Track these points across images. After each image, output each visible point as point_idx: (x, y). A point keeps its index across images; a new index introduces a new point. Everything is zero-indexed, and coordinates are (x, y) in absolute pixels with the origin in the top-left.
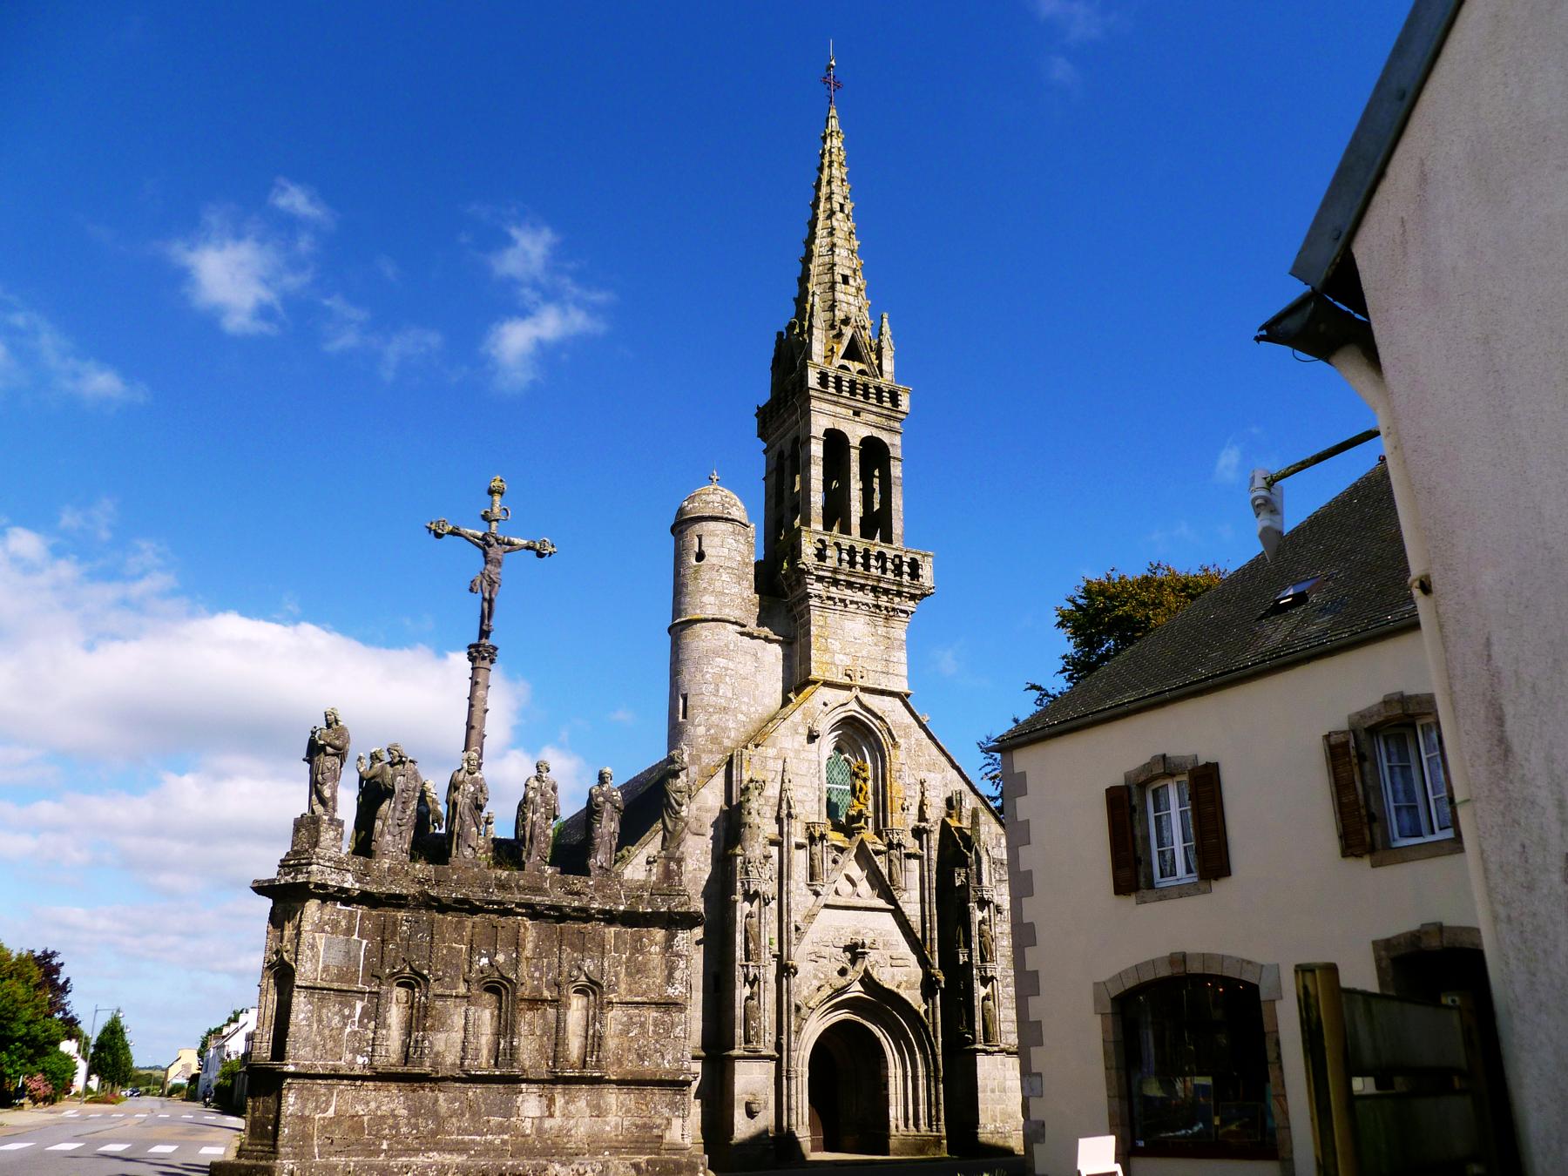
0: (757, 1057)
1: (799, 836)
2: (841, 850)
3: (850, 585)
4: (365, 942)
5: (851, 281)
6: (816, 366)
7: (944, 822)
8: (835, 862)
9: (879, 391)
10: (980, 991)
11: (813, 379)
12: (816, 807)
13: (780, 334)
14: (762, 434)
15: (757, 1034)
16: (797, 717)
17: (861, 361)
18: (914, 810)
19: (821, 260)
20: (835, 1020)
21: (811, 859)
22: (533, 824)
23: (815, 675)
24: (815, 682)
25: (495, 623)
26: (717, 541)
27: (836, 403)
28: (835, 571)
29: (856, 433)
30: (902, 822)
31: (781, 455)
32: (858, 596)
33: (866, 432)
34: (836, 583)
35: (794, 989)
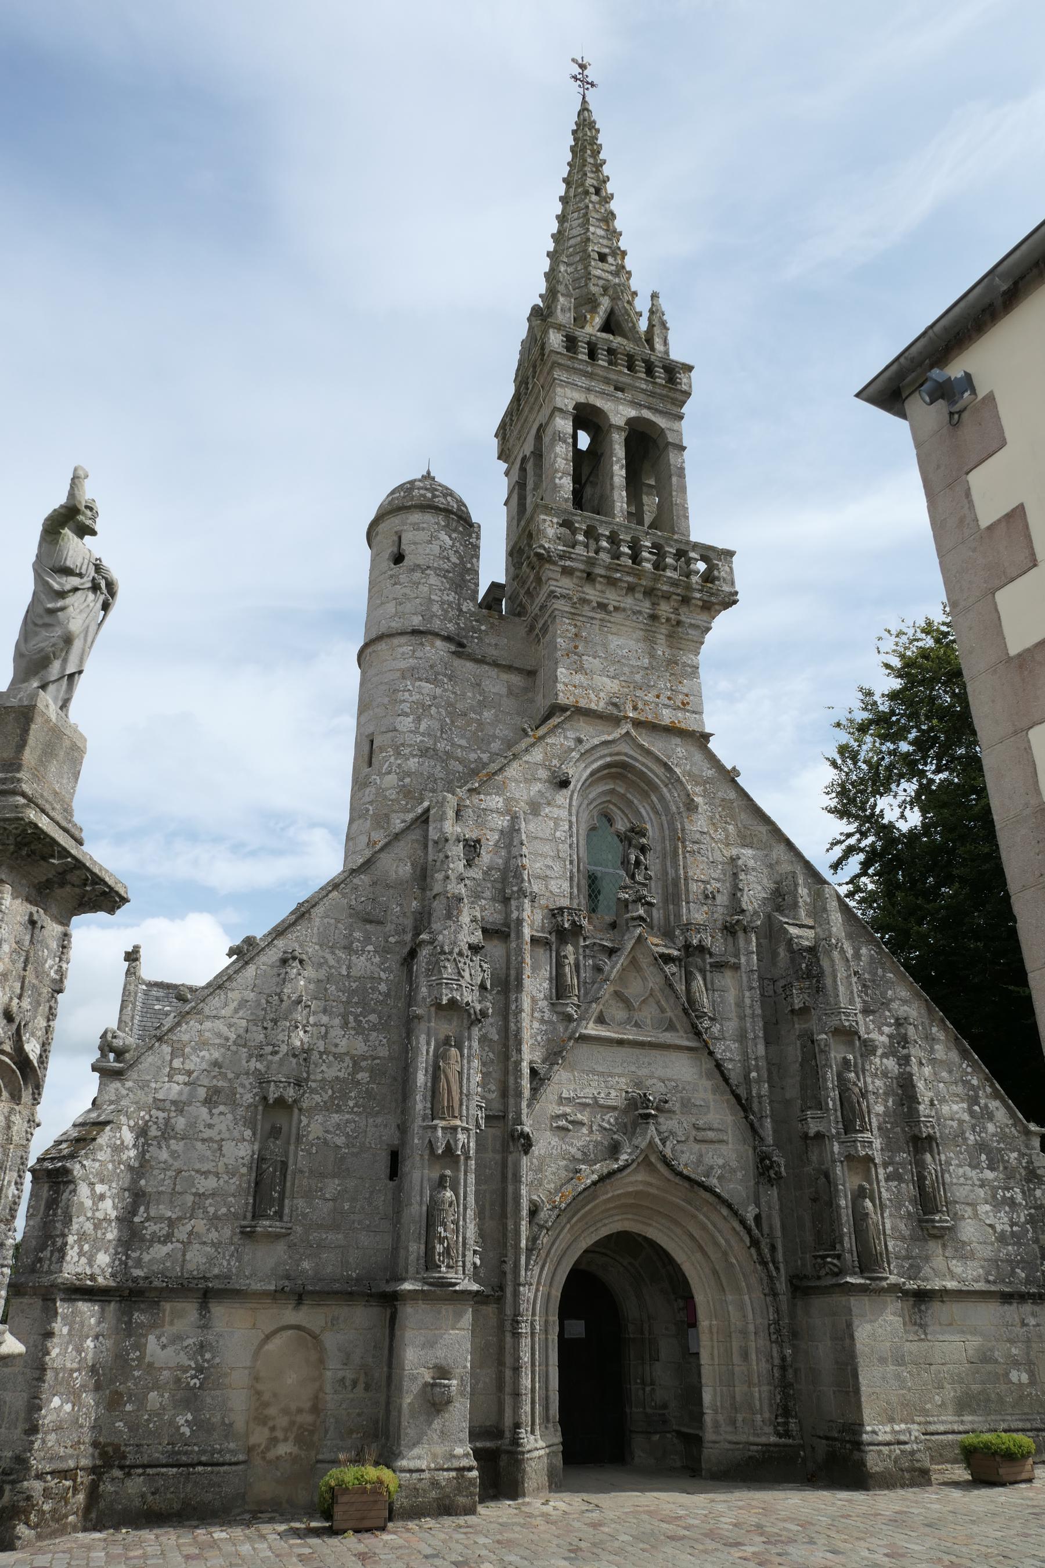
0: (442, 1293)
1: (532, 921)
3: (612, 582)
5: (610, 259)
6: (559, 327)
7: (769, 917)
10: (847, 1182)
12: (566, 885)
15: (447, 1251)
16: (537, 755)
17: (625, 336)
18: (722, 899)
20: (604, 1232)
21: (559, 966)
23: (562, 699)
27: (590, 376)
28: (591, 562)
29: (619, 413)
32: (628, 602)
33: (633, 413)
34: (590, 577)
35: (527, 1175)
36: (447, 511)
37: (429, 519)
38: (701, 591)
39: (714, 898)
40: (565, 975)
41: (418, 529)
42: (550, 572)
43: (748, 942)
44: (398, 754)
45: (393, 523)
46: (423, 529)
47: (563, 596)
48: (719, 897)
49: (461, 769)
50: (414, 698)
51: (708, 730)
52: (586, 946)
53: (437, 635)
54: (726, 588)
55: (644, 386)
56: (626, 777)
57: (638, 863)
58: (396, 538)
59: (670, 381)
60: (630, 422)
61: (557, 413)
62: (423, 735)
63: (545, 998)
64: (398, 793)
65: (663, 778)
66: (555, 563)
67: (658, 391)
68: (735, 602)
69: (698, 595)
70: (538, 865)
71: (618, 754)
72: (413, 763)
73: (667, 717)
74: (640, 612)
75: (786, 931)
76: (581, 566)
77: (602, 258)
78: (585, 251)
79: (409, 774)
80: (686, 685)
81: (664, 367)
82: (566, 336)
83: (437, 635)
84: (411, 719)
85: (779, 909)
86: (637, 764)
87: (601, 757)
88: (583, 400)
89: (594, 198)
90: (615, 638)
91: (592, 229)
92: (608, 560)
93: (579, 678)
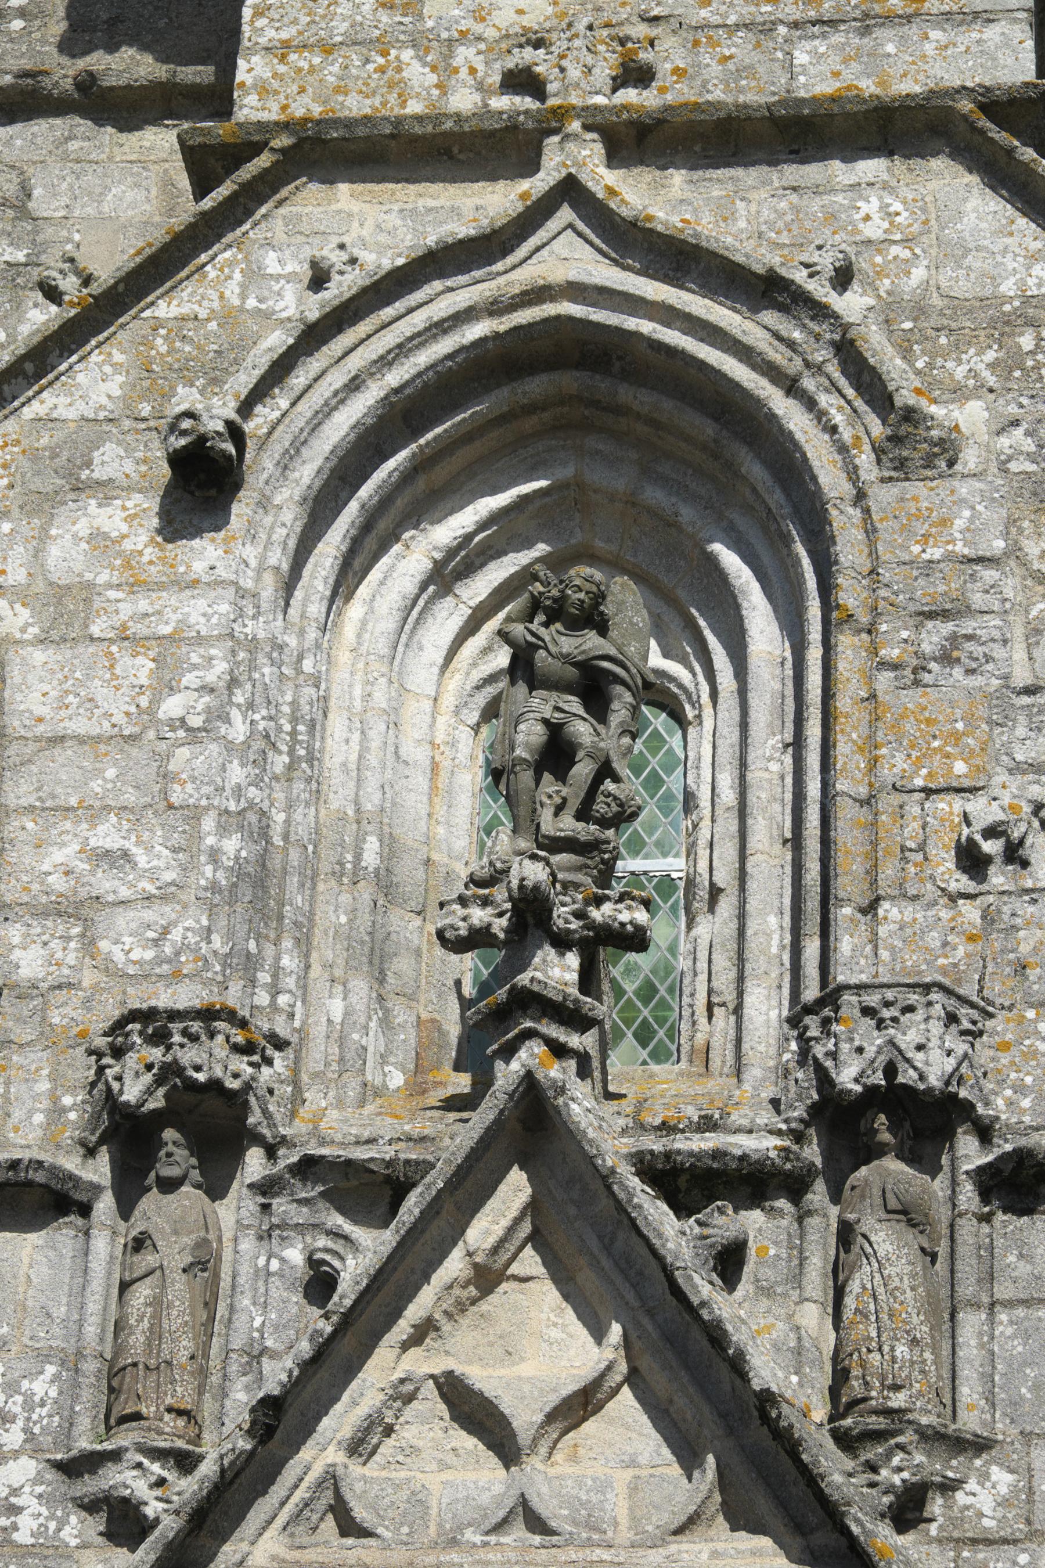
56: (620, 411)
63: (32, 1445)
65: (777, 355)
70: (58, 856)
86: (632, 323)
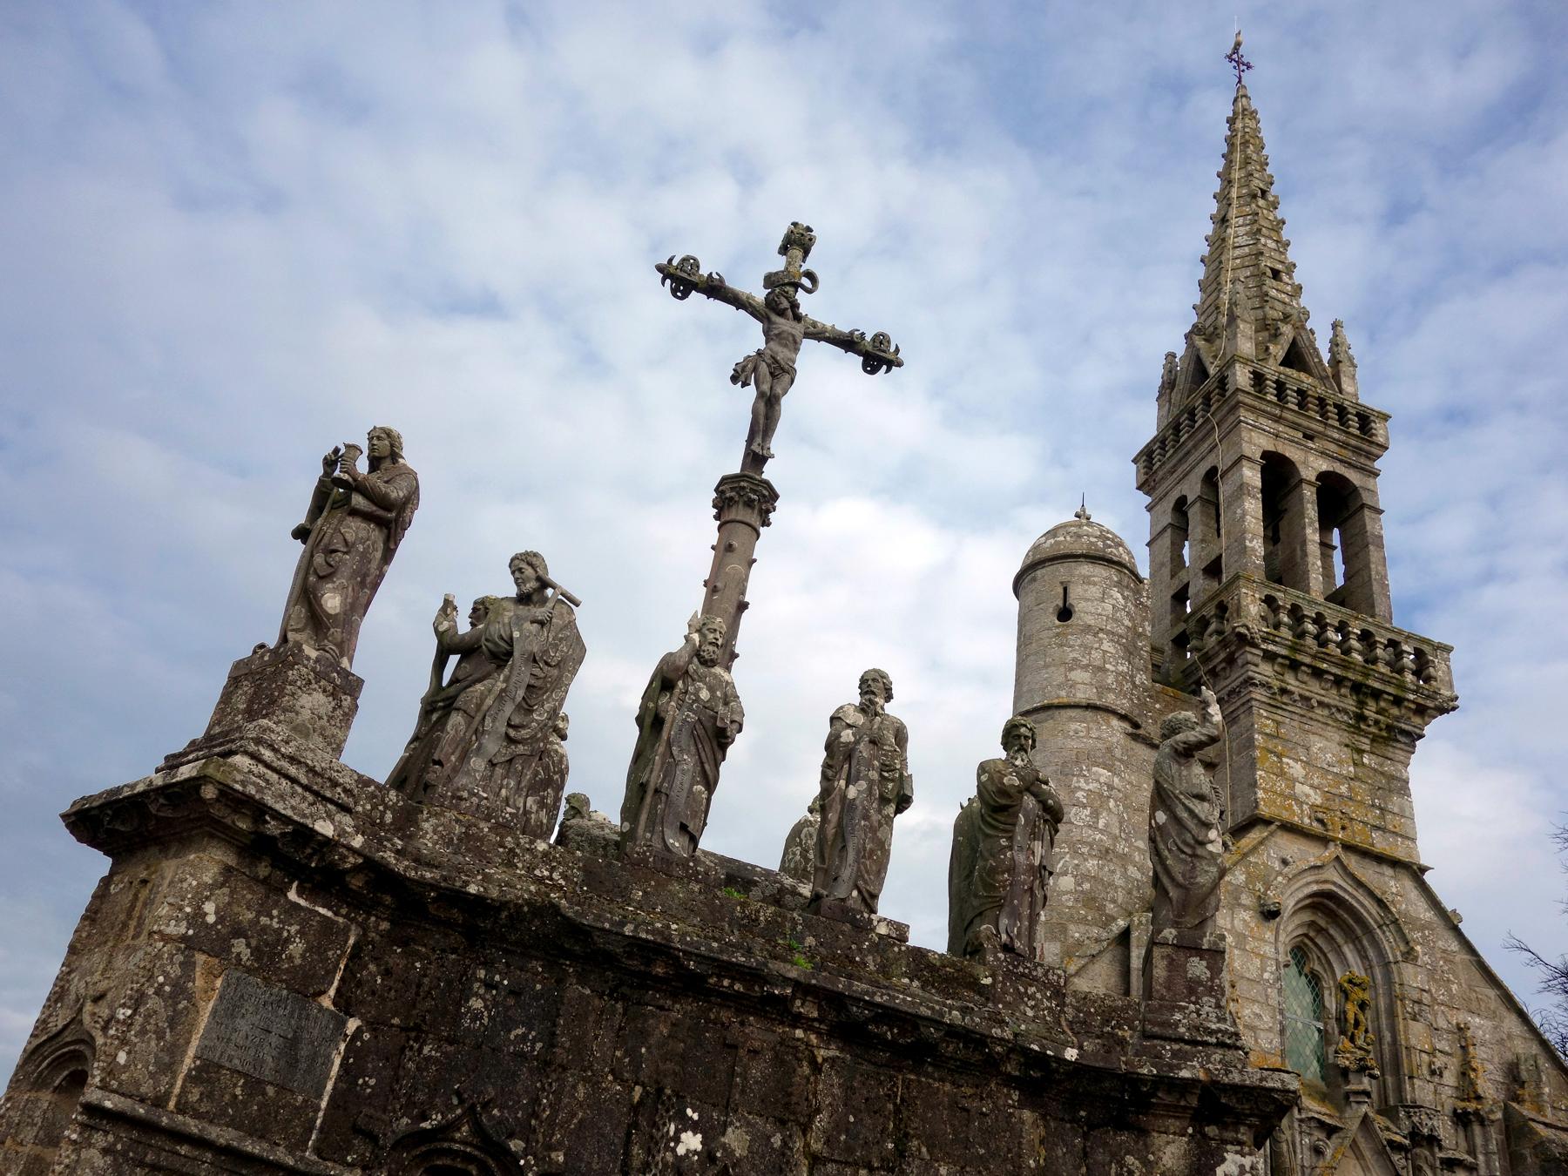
2: (1331, 1131)
3: (1318, 674)
4: (353, 1025)
5: (1285, 278)
6: (1246, 361)
8: (1318, 1151)
9: (1342, 411)
11: (1241, 377)
13: (1171, 356)
14: (1146, 485)
18: (1450, 1078)
19: (1238, 252)
22: (848, 806)
23: (1265, 810)
24: (1267, 822)
25: (777, 444)
26: (1094, 591)
27: (1278, 419)
29: (1311, 465)
30: (1433, 1096)
31: (1181, 506)
32: (1332, 697)
33: (1324, 466)
34: (1294, 666)
36: (1118, 564)
37: (1099, 572)
38: (1415, 692)
39: (1441, 1075)
40: (1281, 1154)
41: (1089, 583)
42: (1253, 655)
43: (1487, 1140)
44: (1075, 853)
45: (1061, 570)
46: (1095, 584)
47: (1263, 685)
48: (1446, 1074)
49: (1139, 876)
50: (1091, 787)
51: (1424, 862)
52: (1301, 1121)
53: (1114, 713)
54: (1445, 692)
55: (1336, 436)
57: (1357, 1024)
58: (1060, 590)
59: (1362, 430)
60: (1322, 476)
61: (1244, 462)
62: (1101, 831)
64: (1076, 900)
66: (1256, 646)
67: (1353, 442)
68: (1454, 709)
69: (1411, 697)
71: (1326, 882)
72: (1091, 864)
73: (1380, 843)
74: (1346, 712)
75: (1533, 1132)
76: (1284, 652)
77: (1276, 274)
78: (1256, 265)
79: (1086, 877)
80: (1395, 803)
81: (1357, 415)
82: (1254, 373)
83: (1114, 713)
84: (1087, 812)
85: (1517, 1099)
87: (1308, 884)
88: (1271, 448)
89: (1261, 202)
90: (1317, 738)
91: (1263, 240)
92: (1315, 648)
93: (1281, 785)
